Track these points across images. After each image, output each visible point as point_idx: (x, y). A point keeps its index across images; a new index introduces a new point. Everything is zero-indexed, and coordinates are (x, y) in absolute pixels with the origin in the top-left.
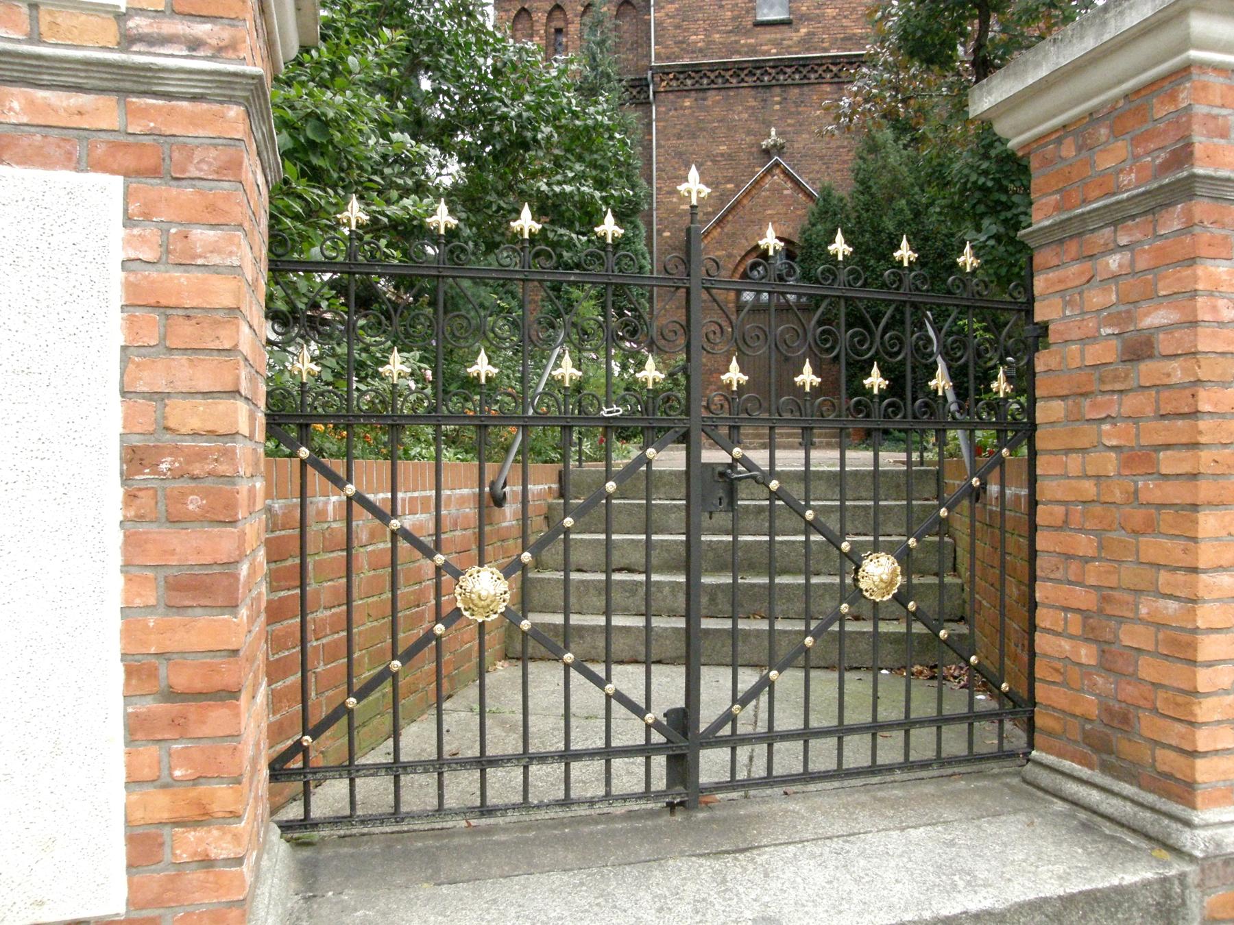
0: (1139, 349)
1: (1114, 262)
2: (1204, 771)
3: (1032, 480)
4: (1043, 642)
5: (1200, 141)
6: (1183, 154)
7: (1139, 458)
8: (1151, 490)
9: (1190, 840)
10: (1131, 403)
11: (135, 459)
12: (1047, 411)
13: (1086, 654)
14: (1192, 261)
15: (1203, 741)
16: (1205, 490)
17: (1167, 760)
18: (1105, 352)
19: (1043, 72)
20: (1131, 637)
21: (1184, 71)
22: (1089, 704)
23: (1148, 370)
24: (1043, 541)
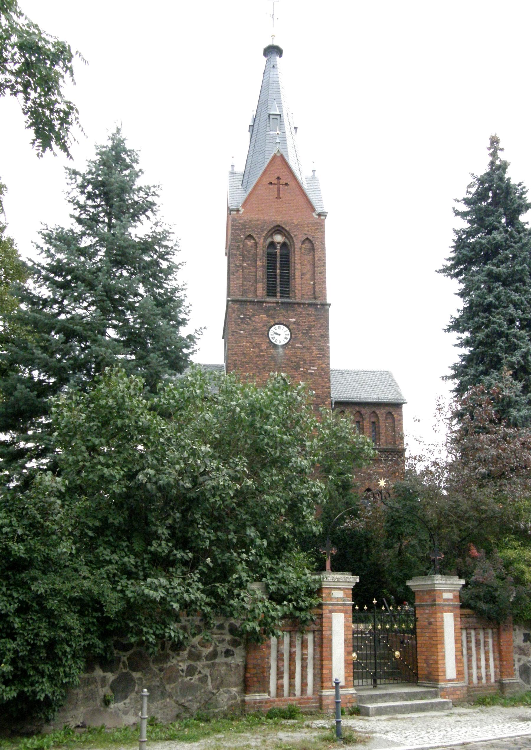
0: (430, 623)
1: (427, 611)
2: (440, 678)
3: (416, 641)
4: (419, 664)
5: (437, 599)
6: (435, 600)
7: (430, 638)
8: (433, 642)
9: (439, 686)
10: (429, 631)
11: (345, 641)
12: (418, 630)
13: (425, 665)
14: (436, 613)
15: (440, 674)
16: (438, 642)
17: (436, 677)
18: (426, 623)
19: (416, 584)
20: (431, 662)
21: (435, 590)
22: (426, 672)
23: (432, 626)
24: (418, 649)
